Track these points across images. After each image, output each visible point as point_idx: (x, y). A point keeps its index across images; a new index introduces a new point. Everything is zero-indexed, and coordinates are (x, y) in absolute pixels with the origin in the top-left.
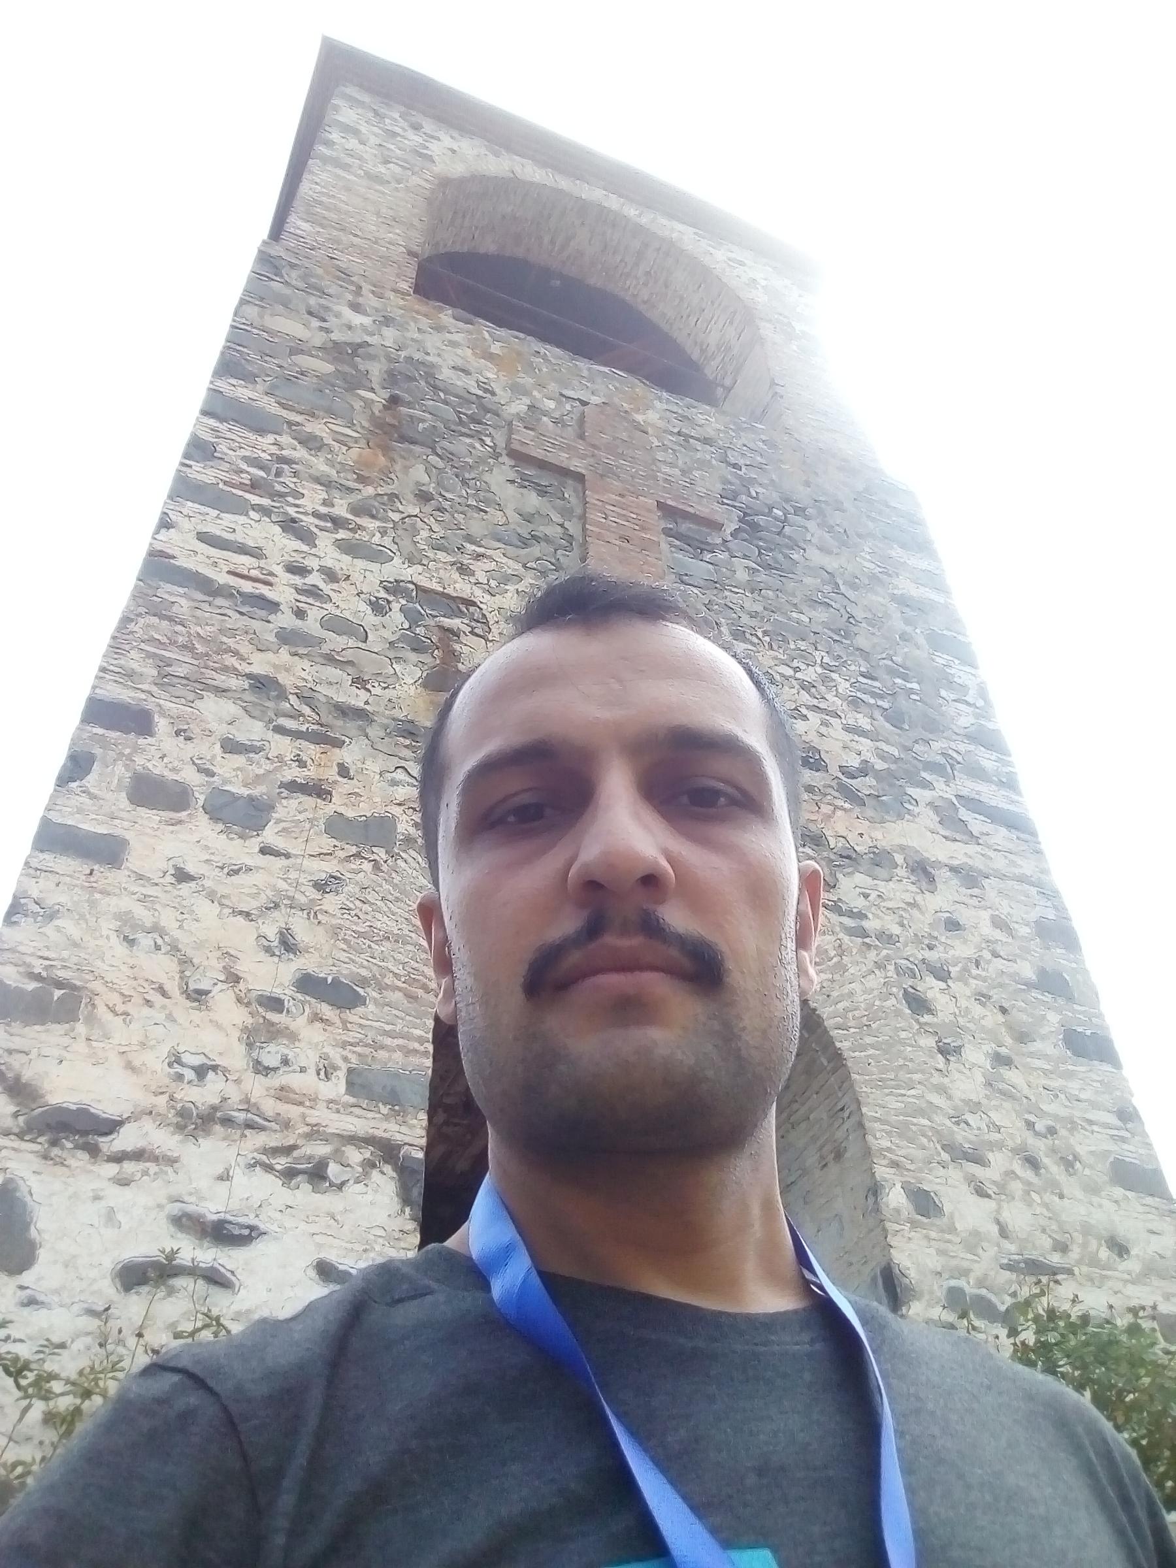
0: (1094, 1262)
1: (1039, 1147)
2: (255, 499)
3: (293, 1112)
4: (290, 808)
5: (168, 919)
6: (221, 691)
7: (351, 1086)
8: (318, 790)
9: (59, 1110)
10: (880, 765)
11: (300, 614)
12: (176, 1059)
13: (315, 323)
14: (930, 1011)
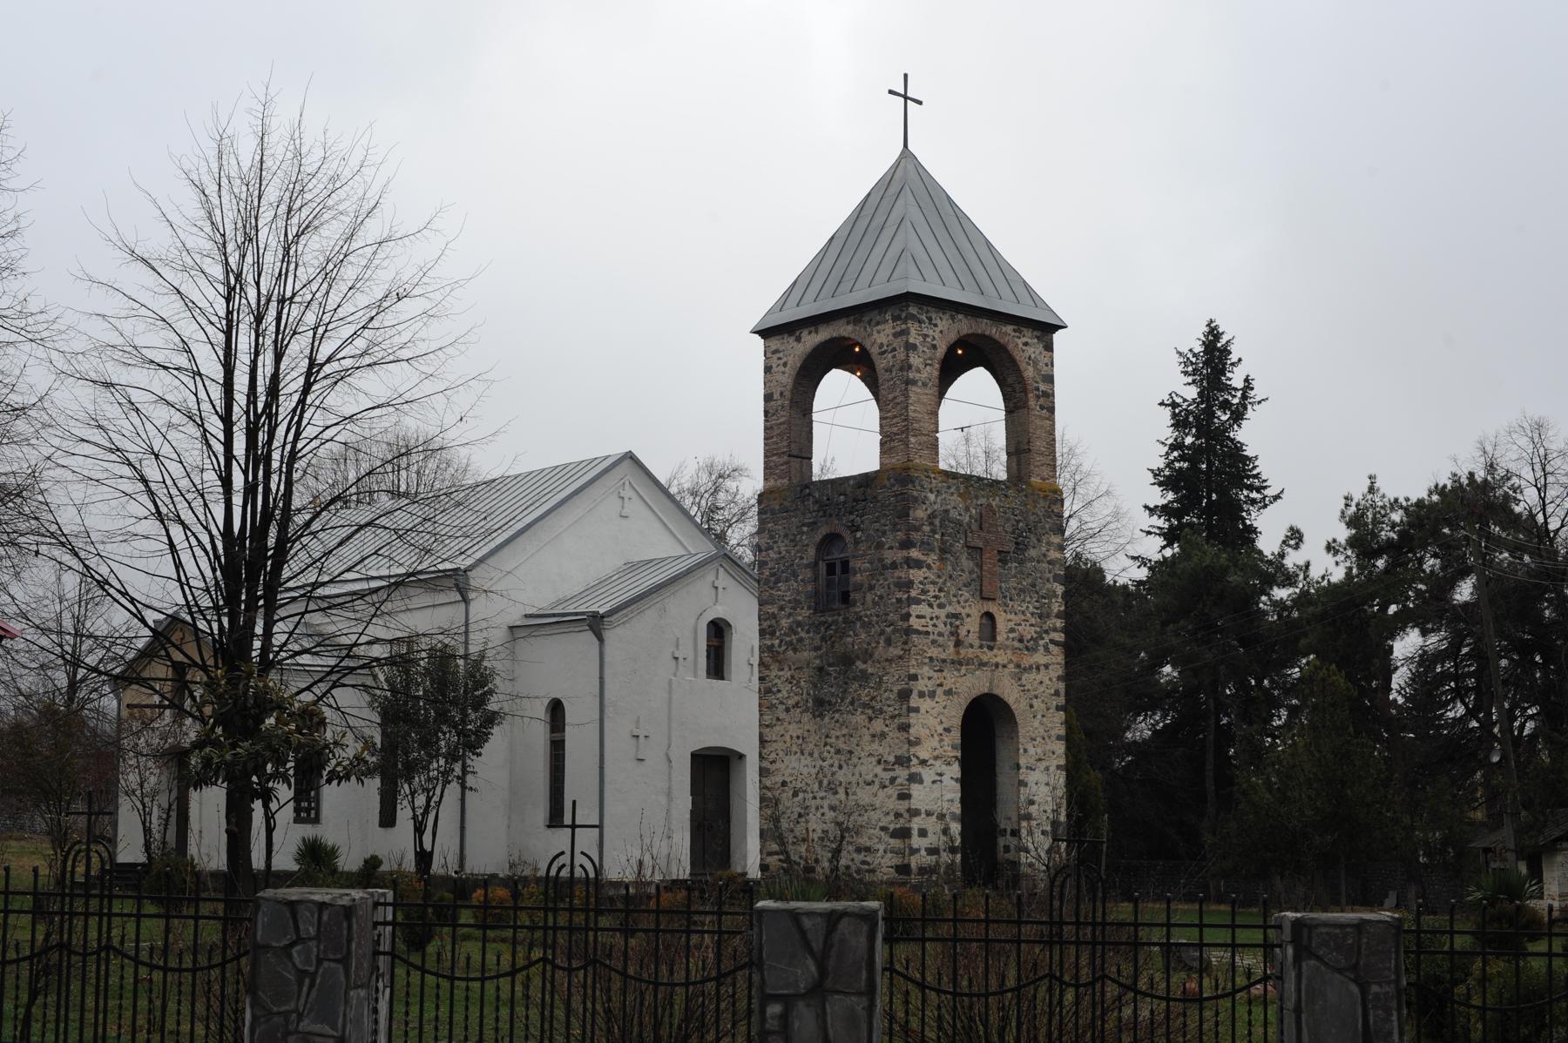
4: (940, 691)
8: (941, 685)
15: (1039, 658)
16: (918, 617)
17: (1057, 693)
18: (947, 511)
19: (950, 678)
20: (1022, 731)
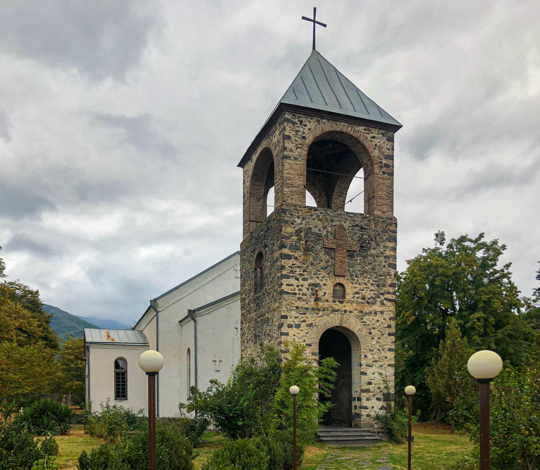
1: (380, 348)
2: (291, 275)
4: (303, 324)
6: (293, 310)
8: (305, 321)
10: (373, 296)
11: (299, 294)
13: (293, 226)
15: (377, 307)
16: (287, 285)
17: (389, 326)
18: (310, 229)
19: (310, 318)
20: (363, 346)
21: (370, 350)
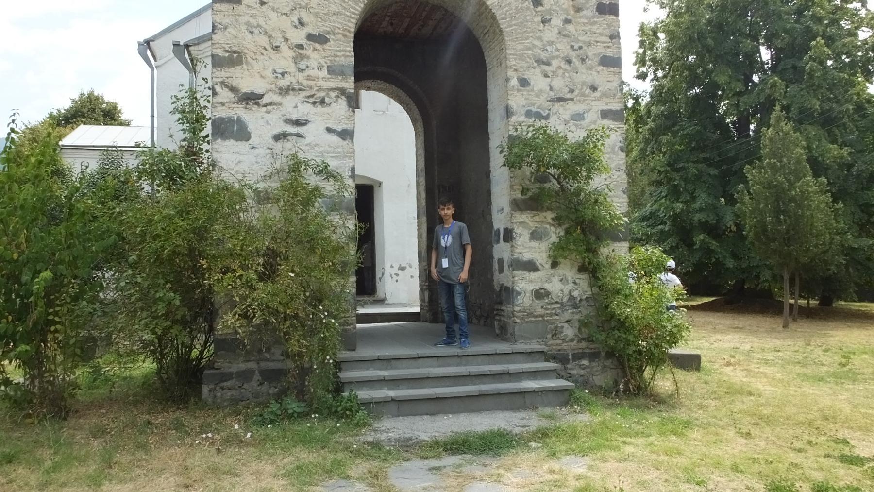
0: (583, 95)
1: (573, 55)
3: (312, 83)
5: (261, 22)
7: (329, 72)
9: (245, 93)
12: (275, 72)
14: (542, 5)
20: (514, 47)
21: (540, 62)
